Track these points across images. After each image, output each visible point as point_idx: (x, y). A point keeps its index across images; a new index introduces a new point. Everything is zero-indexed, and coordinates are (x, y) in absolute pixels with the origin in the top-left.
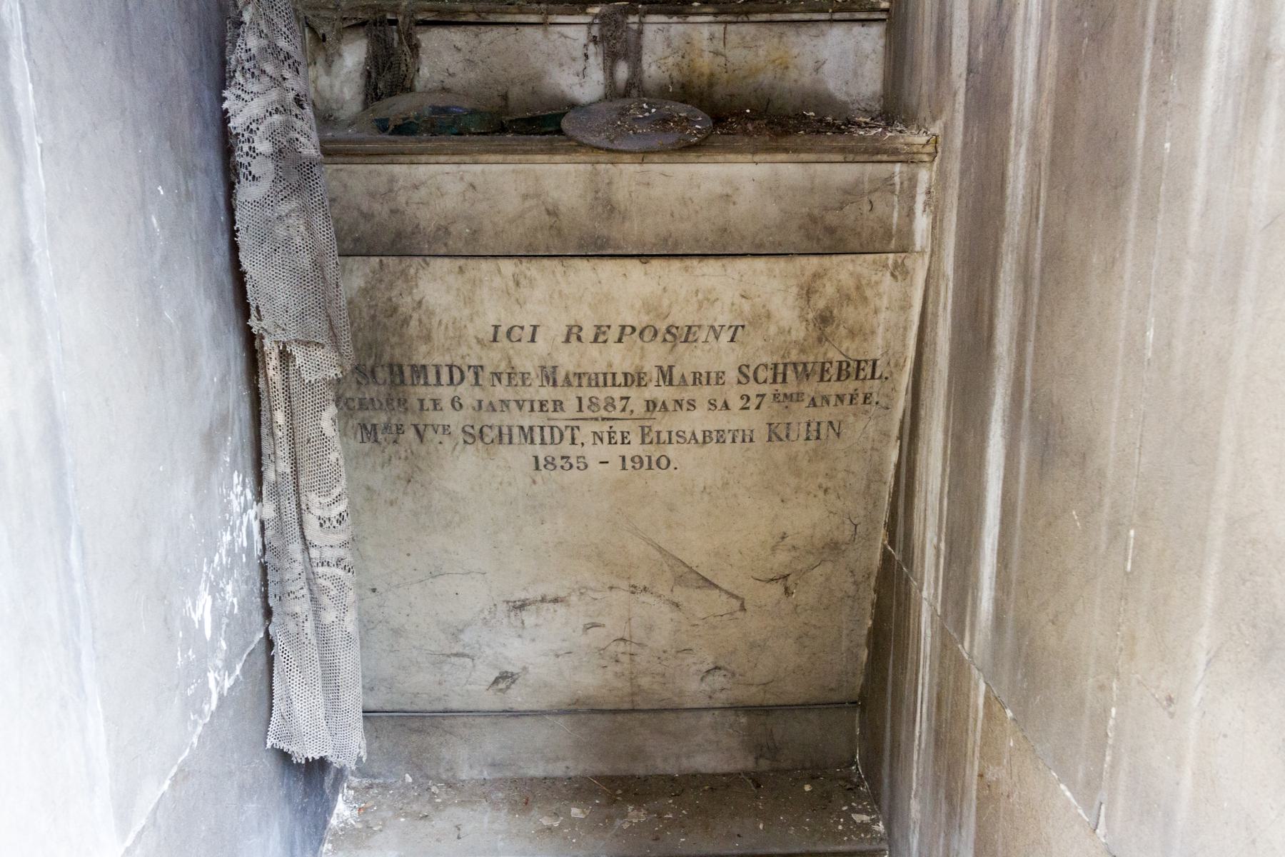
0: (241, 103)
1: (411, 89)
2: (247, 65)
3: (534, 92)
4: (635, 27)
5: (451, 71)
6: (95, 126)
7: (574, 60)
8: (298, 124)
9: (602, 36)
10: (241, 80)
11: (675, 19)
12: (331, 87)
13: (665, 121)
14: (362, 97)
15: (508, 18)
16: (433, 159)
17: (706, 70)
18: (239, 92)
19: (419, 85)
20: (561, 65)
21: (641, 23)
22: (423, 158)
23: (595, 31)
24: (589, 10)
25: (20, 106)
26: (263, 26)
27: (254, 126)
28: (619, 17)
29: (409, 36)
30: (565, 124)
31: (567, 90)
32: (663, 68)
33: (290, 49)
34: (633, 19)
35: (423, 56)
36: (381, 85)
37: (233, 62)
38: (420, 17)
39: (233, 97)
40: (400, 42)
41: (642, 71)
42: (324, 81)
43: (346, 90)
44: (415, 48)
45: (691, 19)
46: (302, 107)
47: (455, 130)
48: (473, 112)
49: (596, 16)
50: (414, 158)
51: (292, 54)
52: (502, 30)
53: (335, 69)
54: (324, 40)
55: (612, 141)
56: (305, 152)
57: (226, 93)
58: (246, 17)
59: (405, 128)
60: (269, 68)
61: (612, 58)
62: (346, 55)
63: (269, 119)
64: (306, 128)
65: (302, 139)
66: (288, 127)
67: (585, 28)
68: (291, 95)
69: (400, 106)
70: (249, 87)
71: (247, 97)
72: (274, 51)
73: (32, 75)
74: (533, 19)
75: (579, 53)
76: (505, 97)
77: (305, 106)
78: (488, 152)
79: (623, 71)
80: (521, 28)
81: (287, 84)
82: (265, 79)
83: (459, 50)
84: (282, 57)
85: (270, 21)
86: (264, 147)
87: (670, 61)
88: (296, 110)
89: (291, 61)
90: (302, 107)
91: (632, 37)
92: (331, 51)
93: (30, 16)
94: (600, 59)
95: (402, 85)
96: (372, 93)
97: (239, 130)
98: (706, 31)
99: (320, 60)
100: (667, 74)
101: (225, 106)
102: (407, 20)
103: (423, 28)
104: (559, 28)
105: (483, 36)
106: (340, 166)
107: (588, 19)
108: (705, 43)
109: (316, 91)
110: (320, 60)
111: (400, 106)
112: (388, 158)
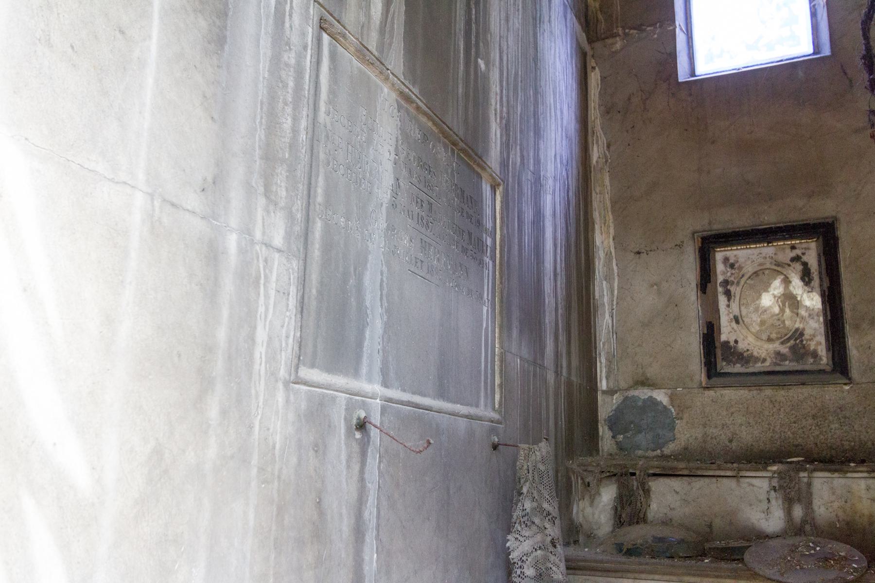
0: (518, 543)
1: (644, 520)
2: (522, 520)
3: (731, 523)
4: (805, 480)
5: (672, 506)
6: (416, 572)
7: (760, 501)
8: (552, 558)
9: (781, 487)
10: (519, 528)
11: (836, 475)
12: (593, 514)
13: (826, 559)
14: (612, 522)
15: (711, 473)
16: (652, 576)
17: (866, 512)
18: (518, 536)
19: (650, 515)
20: (751, 505)
21: (809, 477)
22: (643, 576)
23: (775, 482)
24: (769, 468)
25: (366, 568)
26: (535, 495)
27: (524, 558)
28: (792, 474)
29: (643, 484)
30: (747, 557)
31: (755, 522)
32: (831, 510)
33: (550, 509)
34: (802, 474)
35: (653, 496)
36: (624, 516)
37: (515, 517)
38: (651, 472)
39: (513, 539)
40: (638, 488)
41: (813, 511)
42: (589, 510)
43: (602, 517)
44: (647, 492)
45: (849, 475)
46: (555, 546)
47: (668, 555)
48: (682, 541)
49: (775, 472)
50: (636, 575)
51: (551, 512)
52: (707, 480)
53: (596, 502)
54: (589, 486)
55: (782, 575)
56: (555, 577)
57: (509, 537)
58: (525, 490)
59: (631, 552)
60: (537, 521)
61: (789, 503)
62: (603, 494)
63: (535, 554)
64: (557, 561)
65: (554, 568)
66: (546, 559)
67: (767, 480)
68: (549, 539)
69: (635, 534)
70: (524, 533)
71: (522, 539)
72: (540, 510)
73: (377, 548)
74: (729, 473)
75: (763, 497)
76: (710, 526)
77: (558, 546)
78: (689, 574)
79: (798, 512)
80: (720, 479)
81: (547, 532)
82: (534, 528)
83: (677, 493)
84: (545, 514)
85: (539, 491)
86: (530, 572)
87: (836, 505)
88: (551, 549)
89: (550, 517)
90: (555, 546)
91: (804, 487)
92: (593, 492)
93: (382, 513)
94: (780, 502)
95: (638, 518)
96: (619, 522)
97: (515, 560)
98: (863, 484)
99: (587, 498)
100: (833, 514)
101: (508, 545)
102: (642, 474)
103: (654, 478)
104: (748, 480)
105: (693, 484)
106: (588, 577)
107: (769, 474)
108: (863, 492)
109: (583, 516)
110: (587, 498)
111: (635, 534)
112: (620, 574)
